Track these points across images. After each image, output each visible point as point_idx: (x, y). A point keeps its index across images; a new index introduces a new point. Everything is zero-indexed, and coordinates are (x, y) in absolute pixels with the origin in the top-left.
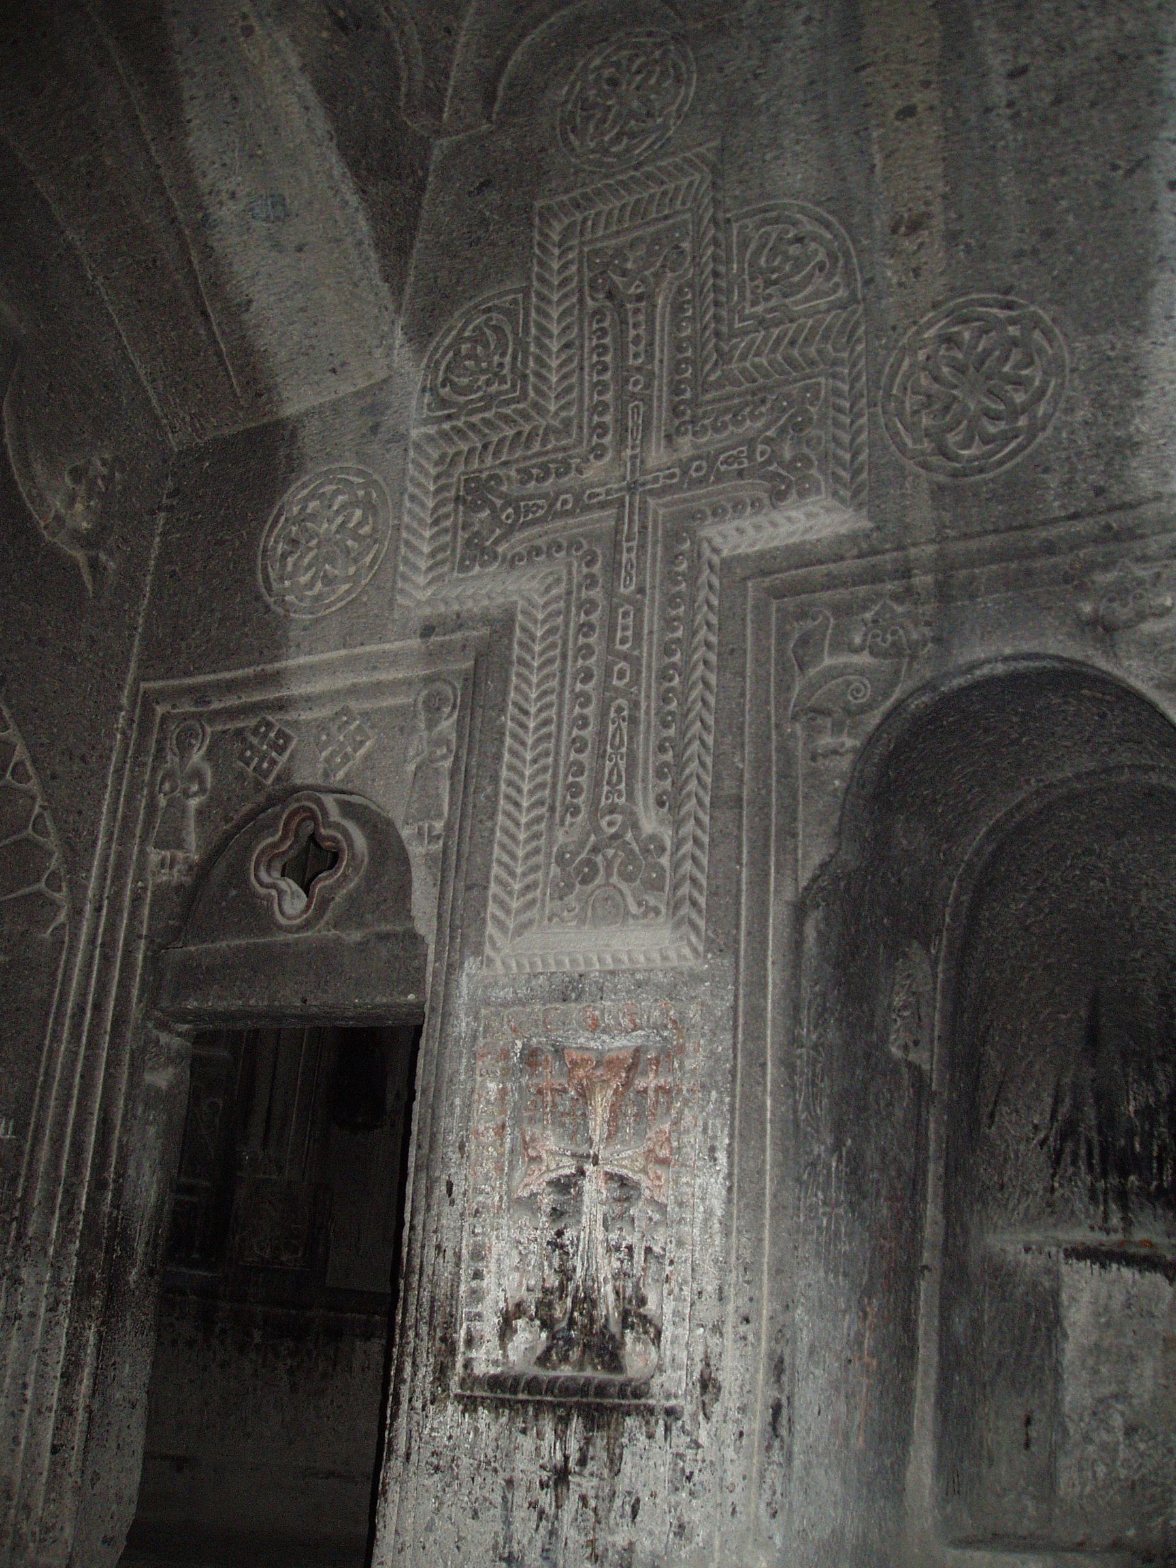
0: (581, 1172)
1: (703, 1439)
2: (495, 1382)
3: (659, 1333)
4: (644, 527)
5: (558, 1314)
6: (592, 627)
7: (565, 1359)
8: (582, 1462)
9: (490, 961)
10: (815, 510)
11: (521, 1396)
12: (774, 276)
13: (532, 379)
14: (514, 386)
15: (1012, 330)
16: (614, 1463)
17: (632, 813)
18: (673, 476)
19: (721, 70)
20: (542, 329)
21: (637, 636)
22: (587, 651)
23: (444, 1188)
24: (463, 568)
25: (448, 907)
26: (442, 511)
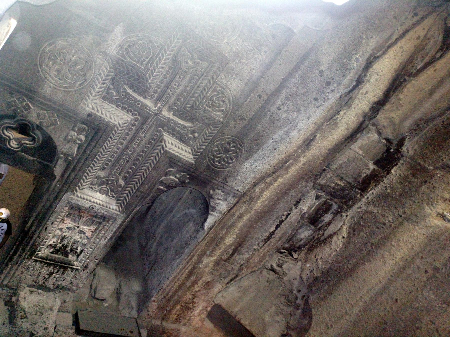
0: (74, 228)
1: (81, 273)
2: (42, 258)
3: (78, 256)
4: (153, 123)
5: (58, 246)
6: (129, 134)
7: (57, 254)
8: (57, 272)
9: (74, 193)
10: (187, 150)
11: (48, 261)
12: (214, 104)
13: (150, 71)
14: (145, 69)
15: (238, 151)
16: (63, 274)
17: (119, 178)
18: (166, 119)
19: (243, 41)
20: (160, 60)
21: (138, 145)
22: (124, 139)
23: (44, 228)
24: (104, 98)
25: (66, 175)
26: (107, 81)
